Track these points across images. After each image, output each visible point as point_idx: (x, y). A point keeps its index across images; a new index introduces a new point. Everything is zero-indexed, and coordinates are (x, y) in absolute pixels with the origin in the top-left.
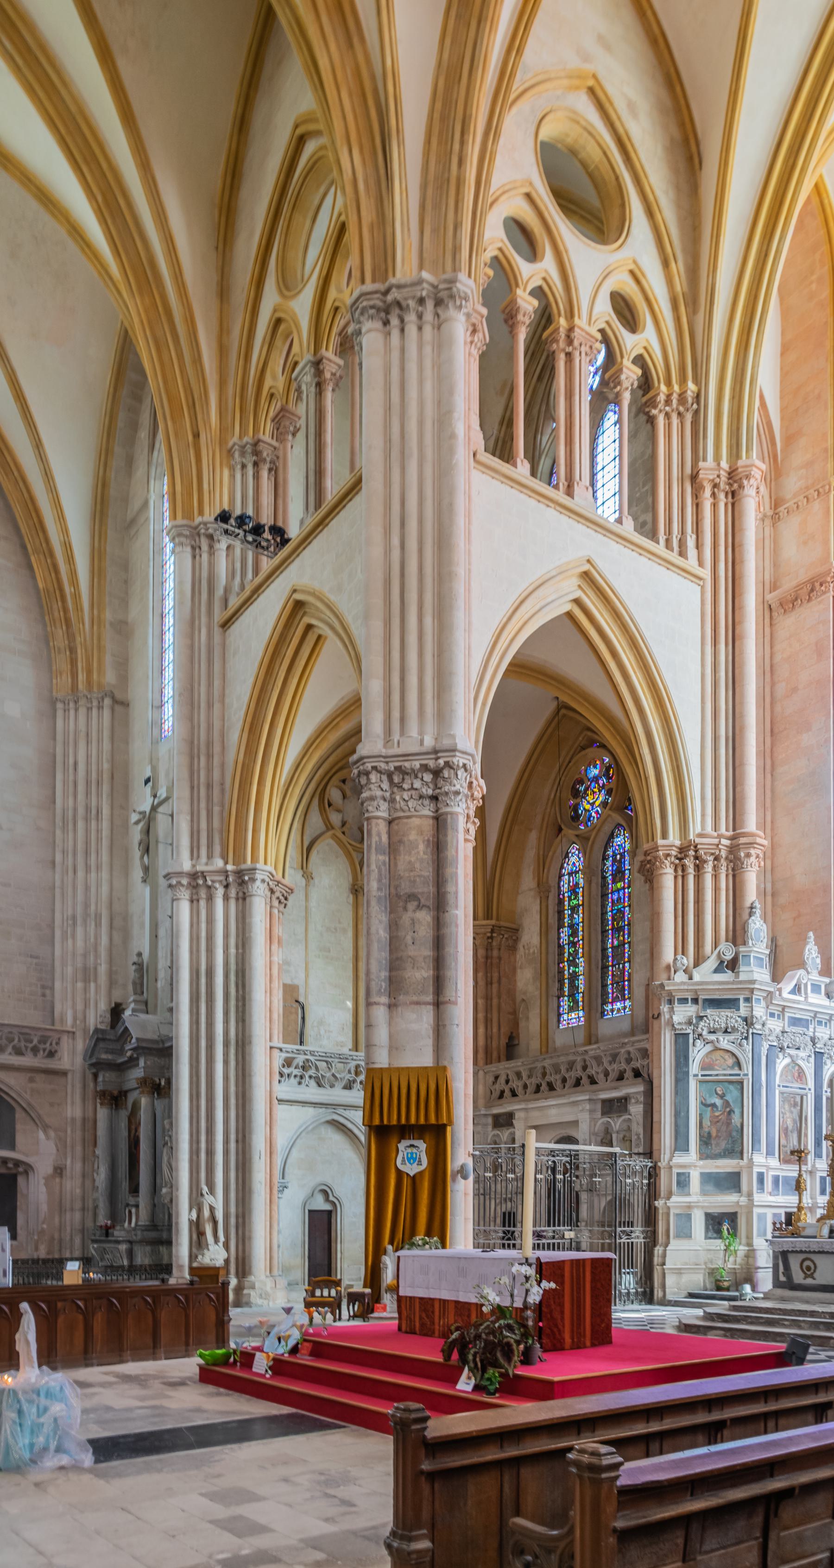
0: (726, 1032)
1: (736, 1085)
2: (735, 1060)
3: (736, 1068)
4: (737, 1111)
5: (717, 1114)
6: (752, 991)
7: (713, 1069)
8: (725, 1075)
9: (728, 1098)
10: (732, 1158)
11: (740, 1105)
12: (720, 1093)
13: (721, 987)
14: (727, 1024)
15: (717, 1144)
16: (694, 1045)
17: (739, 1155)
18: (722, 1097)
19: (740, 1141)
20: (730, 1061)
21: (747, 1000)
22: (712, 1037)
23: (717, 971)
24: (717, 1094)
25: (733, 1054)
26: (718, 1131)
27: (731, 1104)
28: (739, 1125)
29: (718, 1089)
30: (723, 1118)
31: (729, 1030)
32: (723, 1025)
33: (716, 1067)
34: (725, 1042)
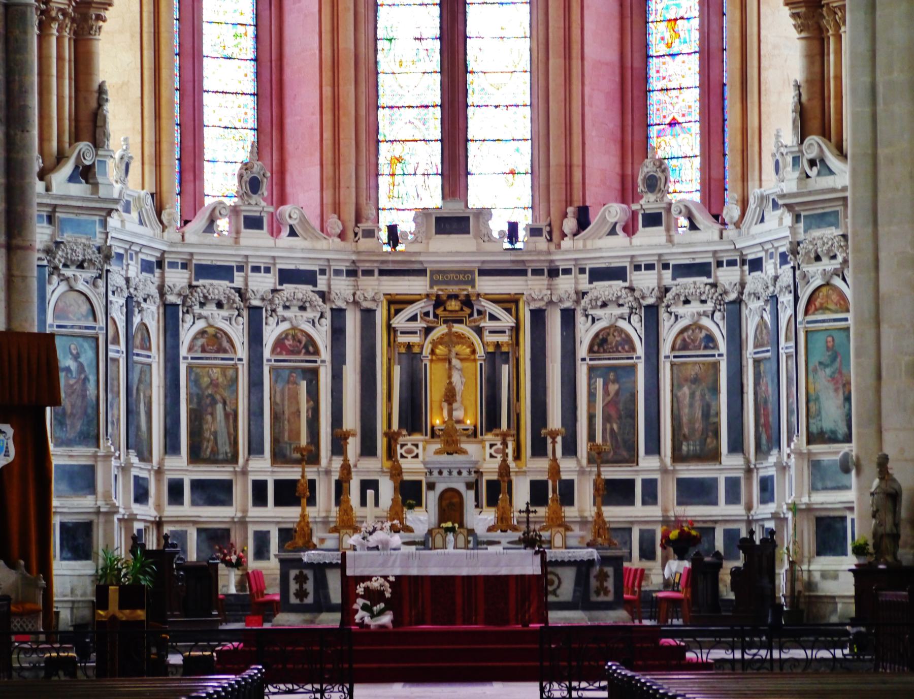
0: (81, 266)
1: (90, 341)
2: (89, 306)
3: (91, 318)
4: (92, 378)
5: (72, 382)
6: (109, 212)
7: (67, 318)
8: (80, 327)
9: (82, 360)
10: (87, 446)
11: (94, 371)
12: (74, 352)
13: (85, 204)
14: (84, 255)
15: (73, 426)
16: (50, 283)
17: (94, 441)
18: (76, 357)
19: (95, 422)
20: (85, 307)
21: (104, 224)
22: (68, 272)
23: (72, 179)
24: (71, 353)
25: (88, 299)
26: (73, 406)
27: (86, 369)
28: (94, 399)
29: (73, 346)
30: (78, 387)
31: (86, 265)
32: (80, 258)
33: (71, 316)
34: (82, 279)
